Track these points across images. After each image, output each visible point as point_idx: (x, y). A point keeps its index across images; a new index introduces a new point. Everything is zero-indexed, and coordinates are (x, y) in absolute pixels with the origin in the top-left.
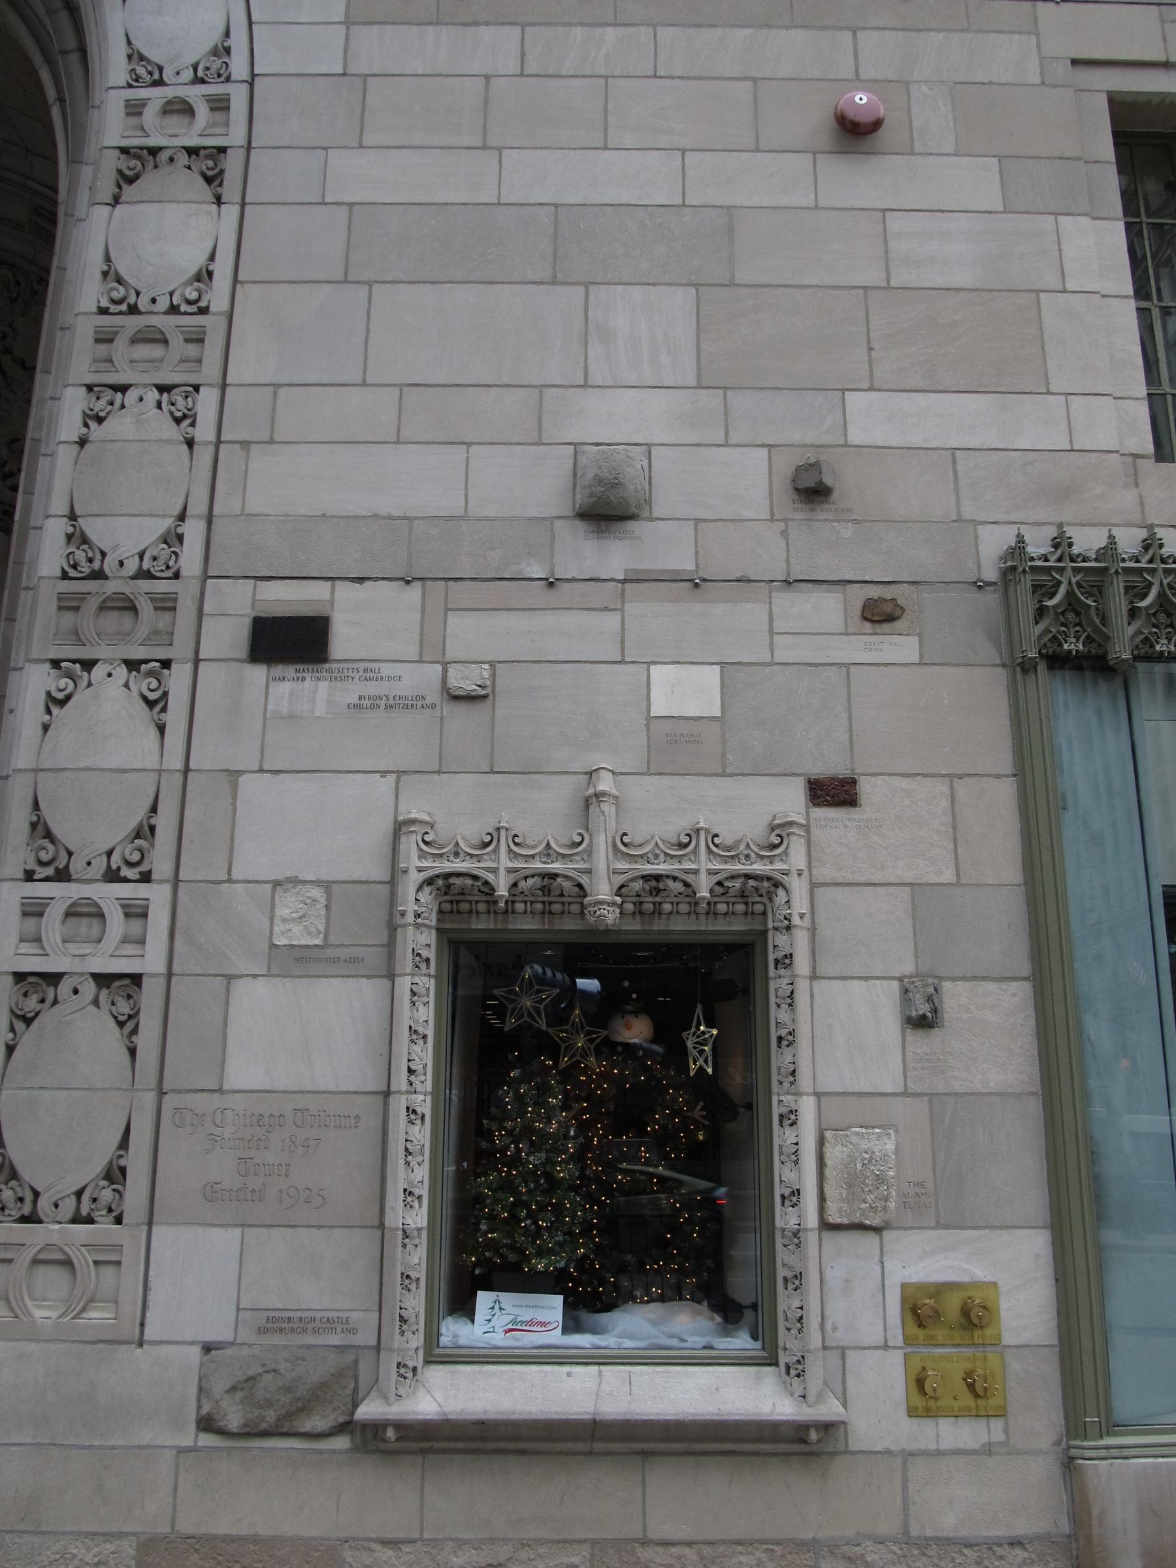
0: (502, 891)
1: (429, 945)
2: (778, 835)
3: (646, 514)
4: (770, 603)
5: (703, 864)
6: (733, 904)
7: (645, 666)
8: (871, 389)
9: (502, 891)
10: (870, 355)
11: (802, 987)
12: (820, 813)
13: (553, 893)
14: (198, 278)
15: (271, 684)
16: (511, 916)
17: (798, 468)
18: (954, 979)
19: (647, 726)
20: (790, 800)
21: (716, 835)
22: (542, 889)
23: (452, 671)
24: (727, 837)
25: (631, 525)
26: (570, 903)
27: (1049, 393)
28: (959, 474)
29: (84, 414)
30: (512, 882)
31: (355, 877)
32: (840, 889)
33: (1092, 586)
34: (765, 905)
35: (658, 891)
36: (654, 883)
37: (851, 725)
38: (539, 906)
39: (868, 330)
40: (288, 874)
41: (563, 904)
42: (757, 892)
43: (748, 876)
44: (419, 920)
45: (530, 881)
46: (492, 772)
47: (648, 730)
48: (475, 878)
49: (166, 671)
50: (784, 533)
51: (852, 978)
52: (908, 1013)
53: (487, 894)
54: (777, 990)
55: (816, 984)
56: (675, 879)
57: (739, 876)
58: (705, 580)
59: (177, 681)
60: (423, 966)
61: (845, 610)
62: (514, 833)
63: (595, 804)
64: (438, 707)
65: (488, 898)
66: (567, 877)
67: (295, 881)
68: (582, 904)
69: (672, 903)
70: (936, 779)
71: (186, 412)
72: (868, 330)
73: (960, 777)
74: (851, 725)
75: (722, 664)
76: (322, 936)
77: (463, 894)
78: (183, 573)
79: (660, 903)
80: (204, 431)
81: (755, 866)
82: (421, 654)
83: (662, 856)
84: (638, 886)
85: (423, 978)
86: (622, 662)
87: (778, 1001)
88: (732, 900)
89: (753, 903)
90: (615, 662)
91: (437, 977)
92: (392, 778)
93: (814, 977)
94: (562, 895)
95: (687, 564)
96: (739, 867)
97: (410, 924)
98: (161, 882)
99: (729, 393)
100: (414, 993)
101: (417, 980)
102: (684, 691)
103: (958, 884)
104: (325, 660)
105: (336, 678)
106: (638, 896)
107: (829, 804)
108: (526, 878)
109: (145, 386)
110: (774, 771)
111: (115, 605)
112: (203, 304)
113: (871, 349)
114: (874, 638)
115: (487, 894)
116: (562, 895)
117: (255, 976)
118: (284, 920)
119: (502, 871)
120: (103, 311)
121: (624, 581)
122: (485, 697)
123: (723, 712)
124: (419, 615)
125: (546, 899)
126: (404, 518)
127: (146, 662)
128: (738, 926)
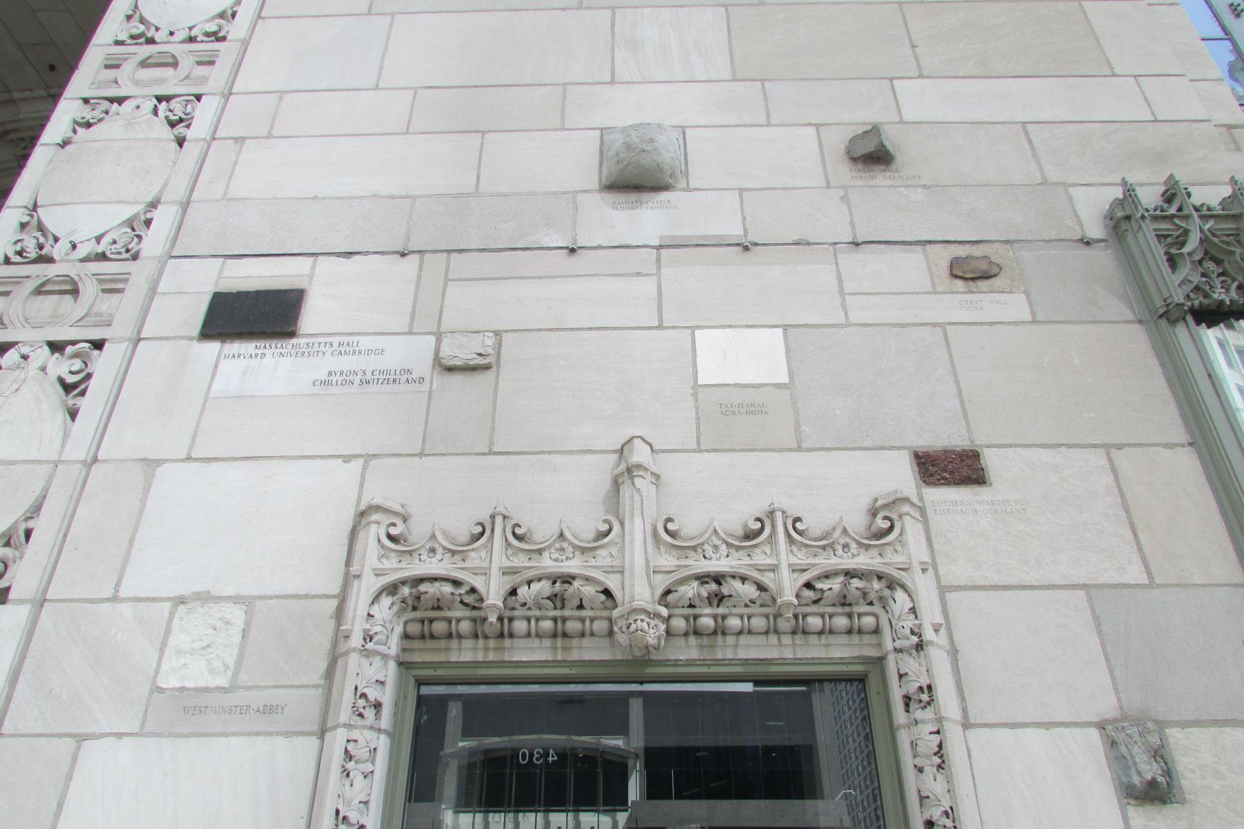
0: (494, 596)
1: (382, 683)
2: (886, 518)
3: (682, 185)
4: (837, 264)
5: (783, 557)
6: (831, 616)
7: (689, 331)
8: (921, 76)
9: (494, 596)
10: (914, 52)
11: (954, 734)
12: (939, 496)
13: (568, 605)
14: (222, 15)
15: (222, 361)
16: (507, 642)
17: (852, 141)
18: (1184, 724)
19: (695, 395)
20: (900, 476)
21: (798, 519)
22: (553, 597)
23: (446, 341)
24: (814, 523)
25: (664, 196)
26: (592, 620)
27: (1114, 75)
28: (1035, 143)
29: (75, 122)
30: (508, 587)
31: (291, 590)
32: (981, 594)
33: (1228, 235)
34: (876, 616)
35: (720, 599)
36: (714, 586)
37: (959, 390)
38: (547, 625)
39: (909, 34)
40: (198, 588)
41: (582, 620)
42: (860, 595)
43: (849, 574)
44: (370, 646)
45: (535, 586)
46: (491, 453)
47: (696, 400)
48: (456, 583)
49: (96, 352)
50: (844, 199)
51: (1025, 725)
52: (1124, 780)
53: (474, 608)
54: (913, 745)
55: (971, 733)
56: (744, 579)
57: (837, 573)
58: (756, 244)
59: (104, 366)
60: (370, 713)
61: (930, 269)
62: (514, 522)
63: (628, 482)
64: (427, 381)
65: (475, 613)
66: (588, 579)
67: (205, 598)
68: (610, 620)
69: (741, 617)
70: (1087, 450)
71: (183, 116)
72: (909, 34)
73: (1119, 447)
74: (959, 390)
75: (786, 328)
76: (230, 673)
77: (439, 608)
78: (143, 254)
79: (724, 617)
80: (198, 131)
81: (857, 560)
82: (411, 325)
83: (724, 547)
84: (690, 590)
85: (367, 733)
86: (660, 327)
87: (918, 761)
88: (830, 610)
89: (860, 615)
90: (651, 328)
91: (393, 735)
92: (357, 465)
93: (967, 725)
94: (581, 607)
95: (734, 230)
96: (834, 560)
97: (355, 650)
98: (21, 601)
99: (767, 84)
100: (349, 756)
101: (355, 734)
102: (741, 356)
103: (1151, 585)
104: (292, 335)
105: (303, 354)
106: (691, 606)
107: (947, 483)
108: (529, 583)
109: (144, 97)
110: (866, 444)
111: (56, 288)
112: (221, 34)
113: (914, 47)
114: (969, 297)
115: (474, 608)
116: (581, 607)
117: (120, 735)
118: (179, 652)
119: (495, 571)
120: (119, 43)
121: (661, 247)
122: (487, 367)
123: (791, 378)
124: (413, 287)
125: (557, 613)
126: (406, 197)
127: (74, 343)
128: (839, 652)
